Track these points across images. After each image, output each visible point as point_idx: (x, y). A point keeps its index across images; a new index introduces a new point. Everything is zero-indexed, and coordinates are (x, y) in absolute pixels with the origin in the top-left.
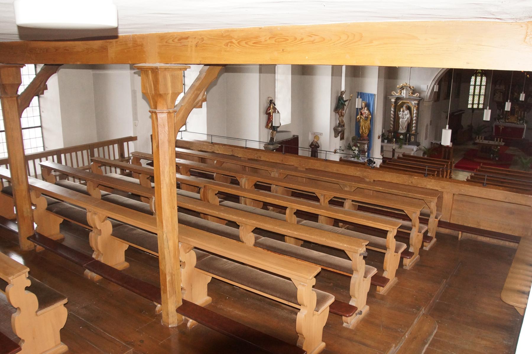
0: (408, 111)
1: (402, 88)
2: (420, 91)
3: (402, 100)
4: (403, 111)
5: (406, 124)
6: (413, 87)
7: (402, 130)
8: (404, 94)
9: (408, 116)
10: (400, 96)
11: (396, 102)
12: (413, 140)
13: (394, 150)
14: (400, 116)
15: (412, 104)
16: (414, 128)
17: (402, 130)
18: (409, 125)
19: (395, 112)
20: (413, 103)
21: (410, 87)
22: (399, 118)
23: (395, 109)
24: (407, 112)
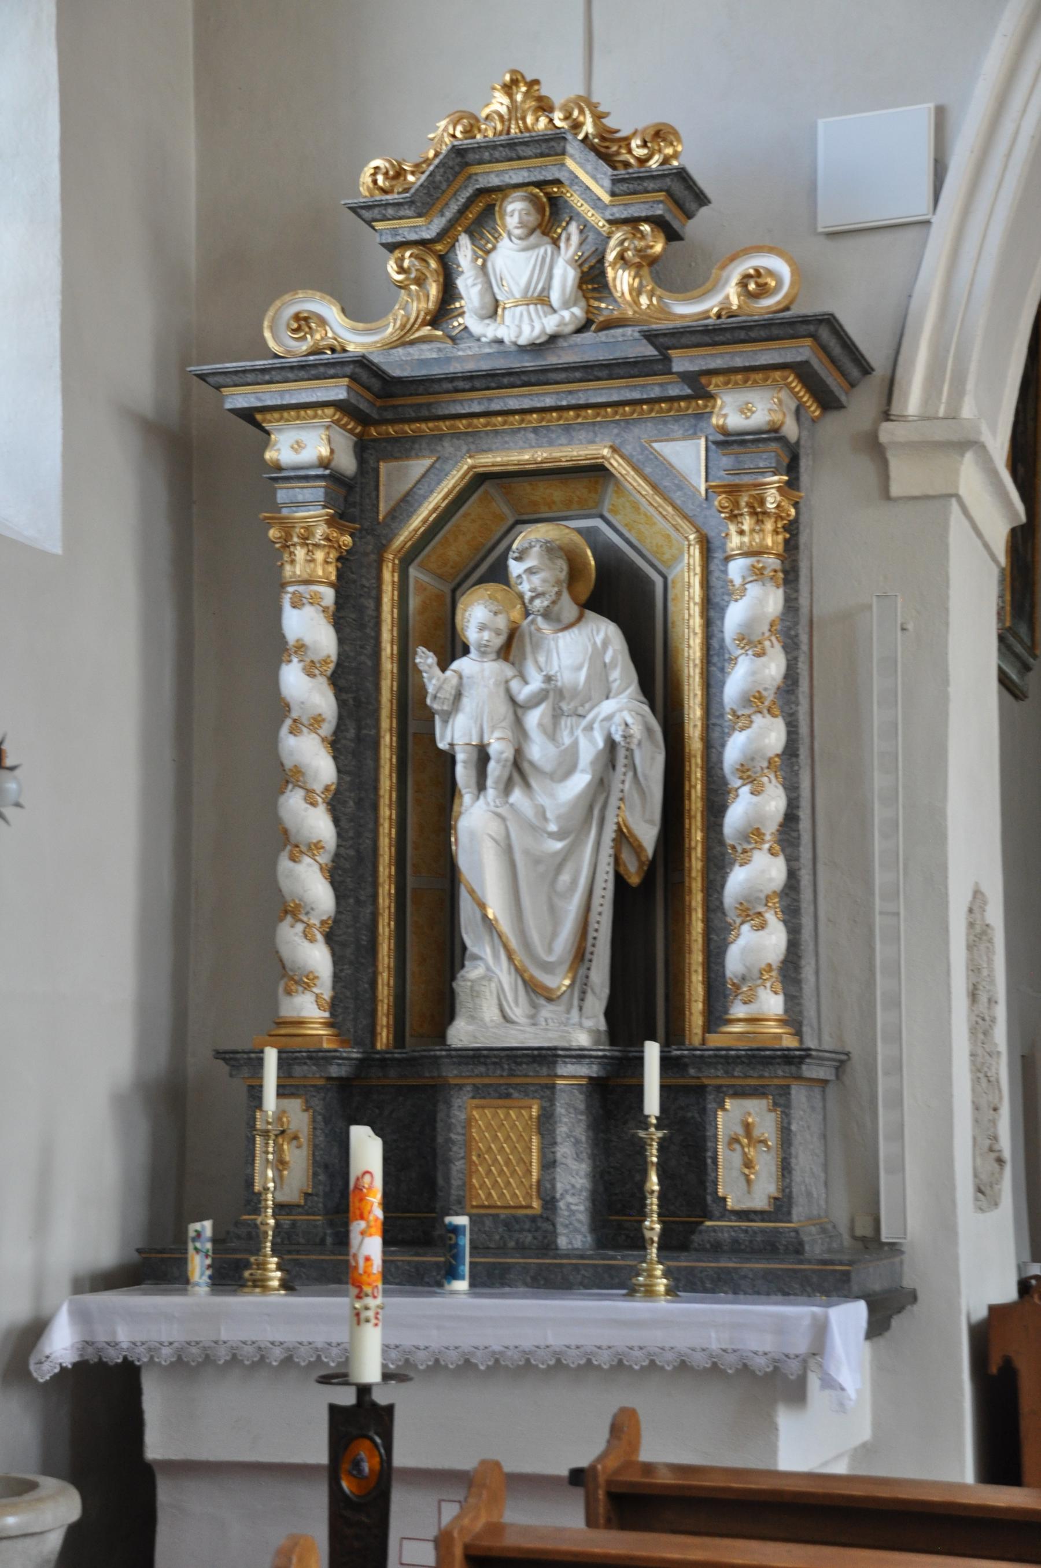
0: (603, 634)
1: (461, 193)
2: (796, 215)
3: (474, 430)
4: (510, 648)
5: (586, 880)
6: (660, 134)
7: (523, 984)
8: (516, 290)
9: (623, 710)
10: (423, 358)
11: (351, 497)
12: (743, 1181)
13: (361, 1423)
14: (456, 733)
15: (664, 481)
16: (757, 945)
17: (523, 984)
18: (651, 915)
19: (352, 678)
20: (687, 456)
21: (605, 148)
22: (433, 784)
23: (352, 613)
24: (584, 650)
